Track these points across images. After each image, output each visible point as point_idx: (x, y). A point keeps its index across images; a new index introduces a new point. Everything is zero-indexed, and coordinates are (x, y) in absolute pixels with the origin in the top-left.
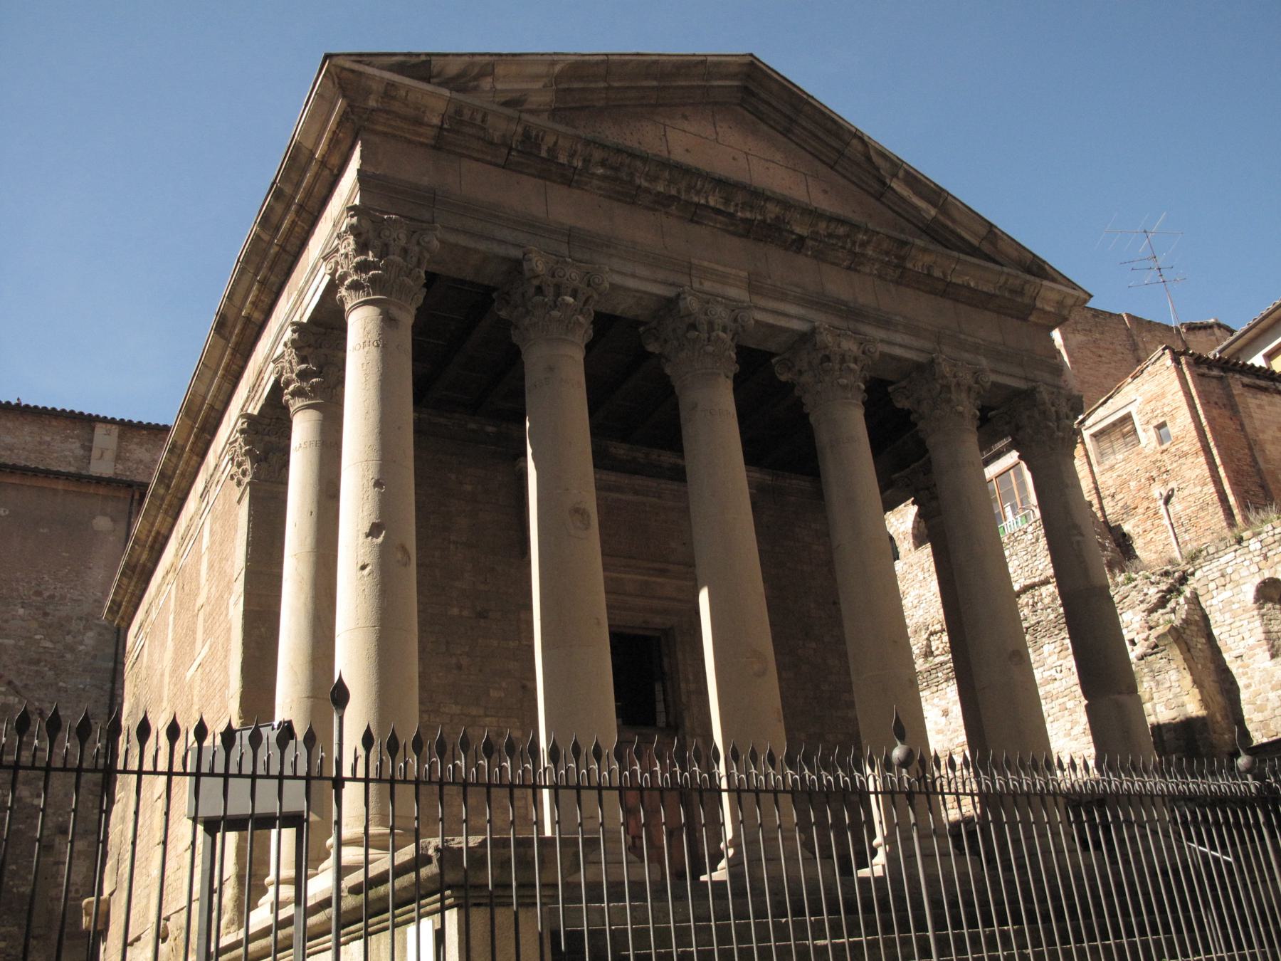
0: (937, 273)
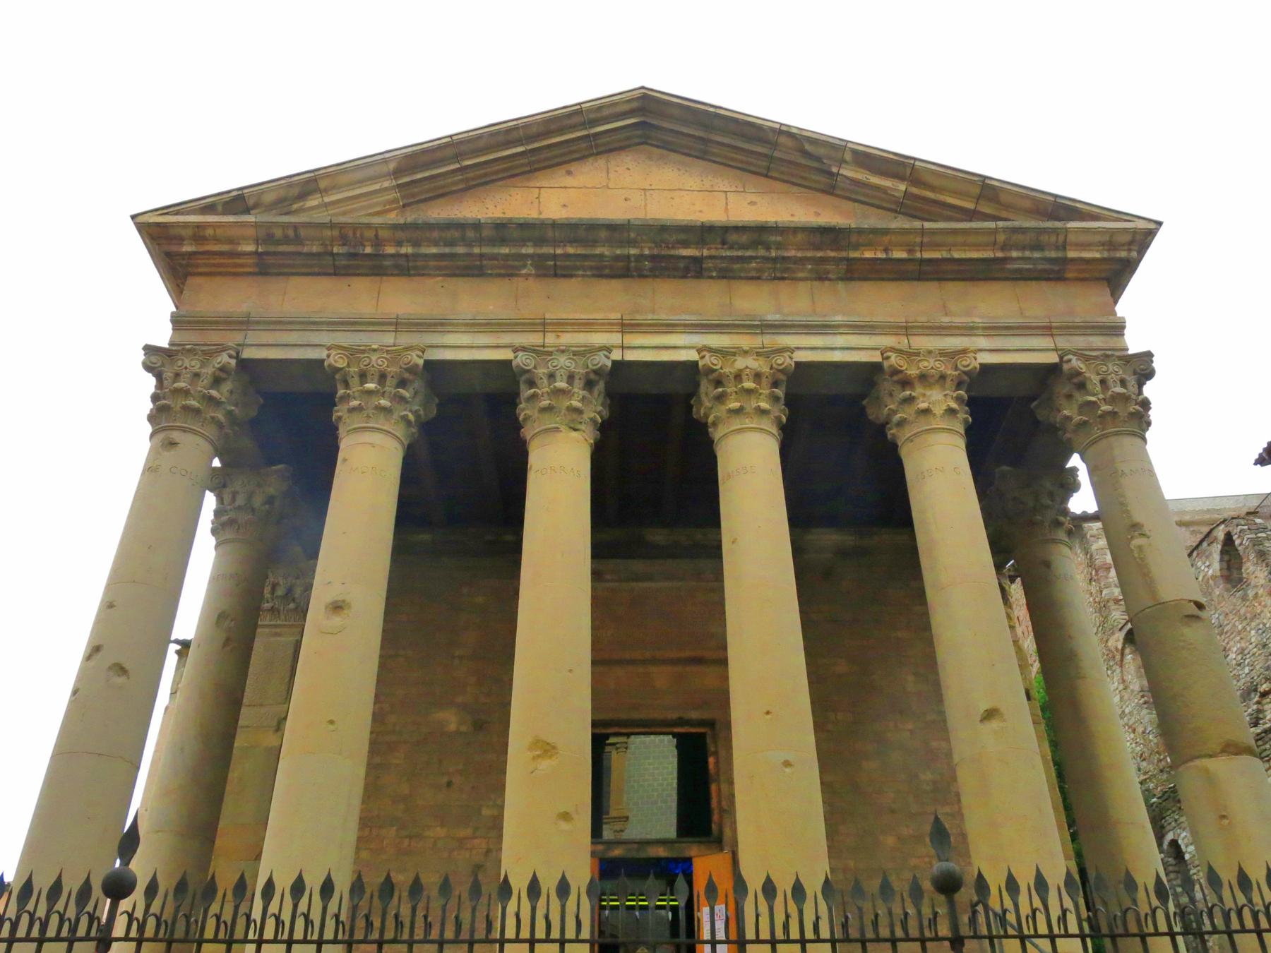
0: (899, 254)
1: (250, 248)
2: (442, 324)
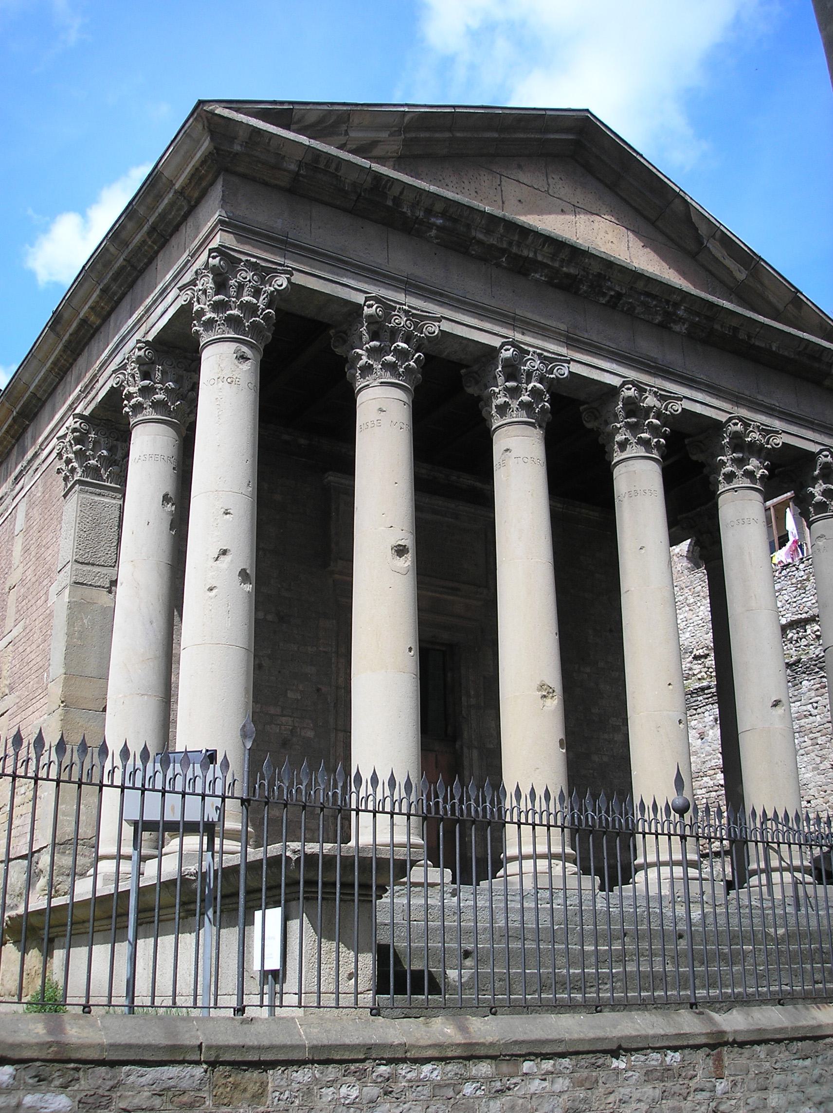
1: (293, 167)
2: (441, 295)
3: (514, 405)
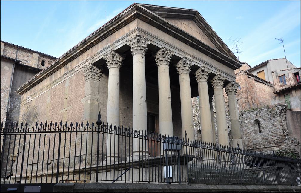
0: (220, 58)
3: (185, 70)
